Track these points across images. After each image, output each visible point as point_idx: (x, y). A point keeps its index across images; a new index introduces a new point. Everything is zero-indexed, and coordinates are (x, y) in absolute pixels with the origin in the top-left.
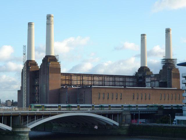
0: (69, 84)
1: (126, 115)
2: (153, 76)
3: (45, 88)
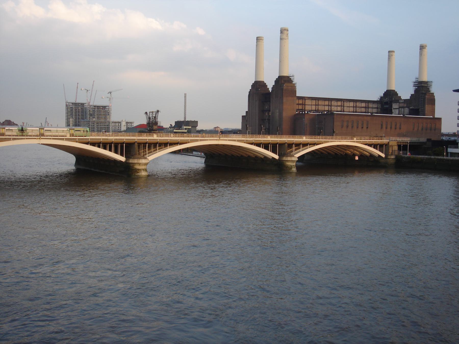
0: (302, 110)
1: (393, 146)
2: (402, 101)
3: (277, 114)
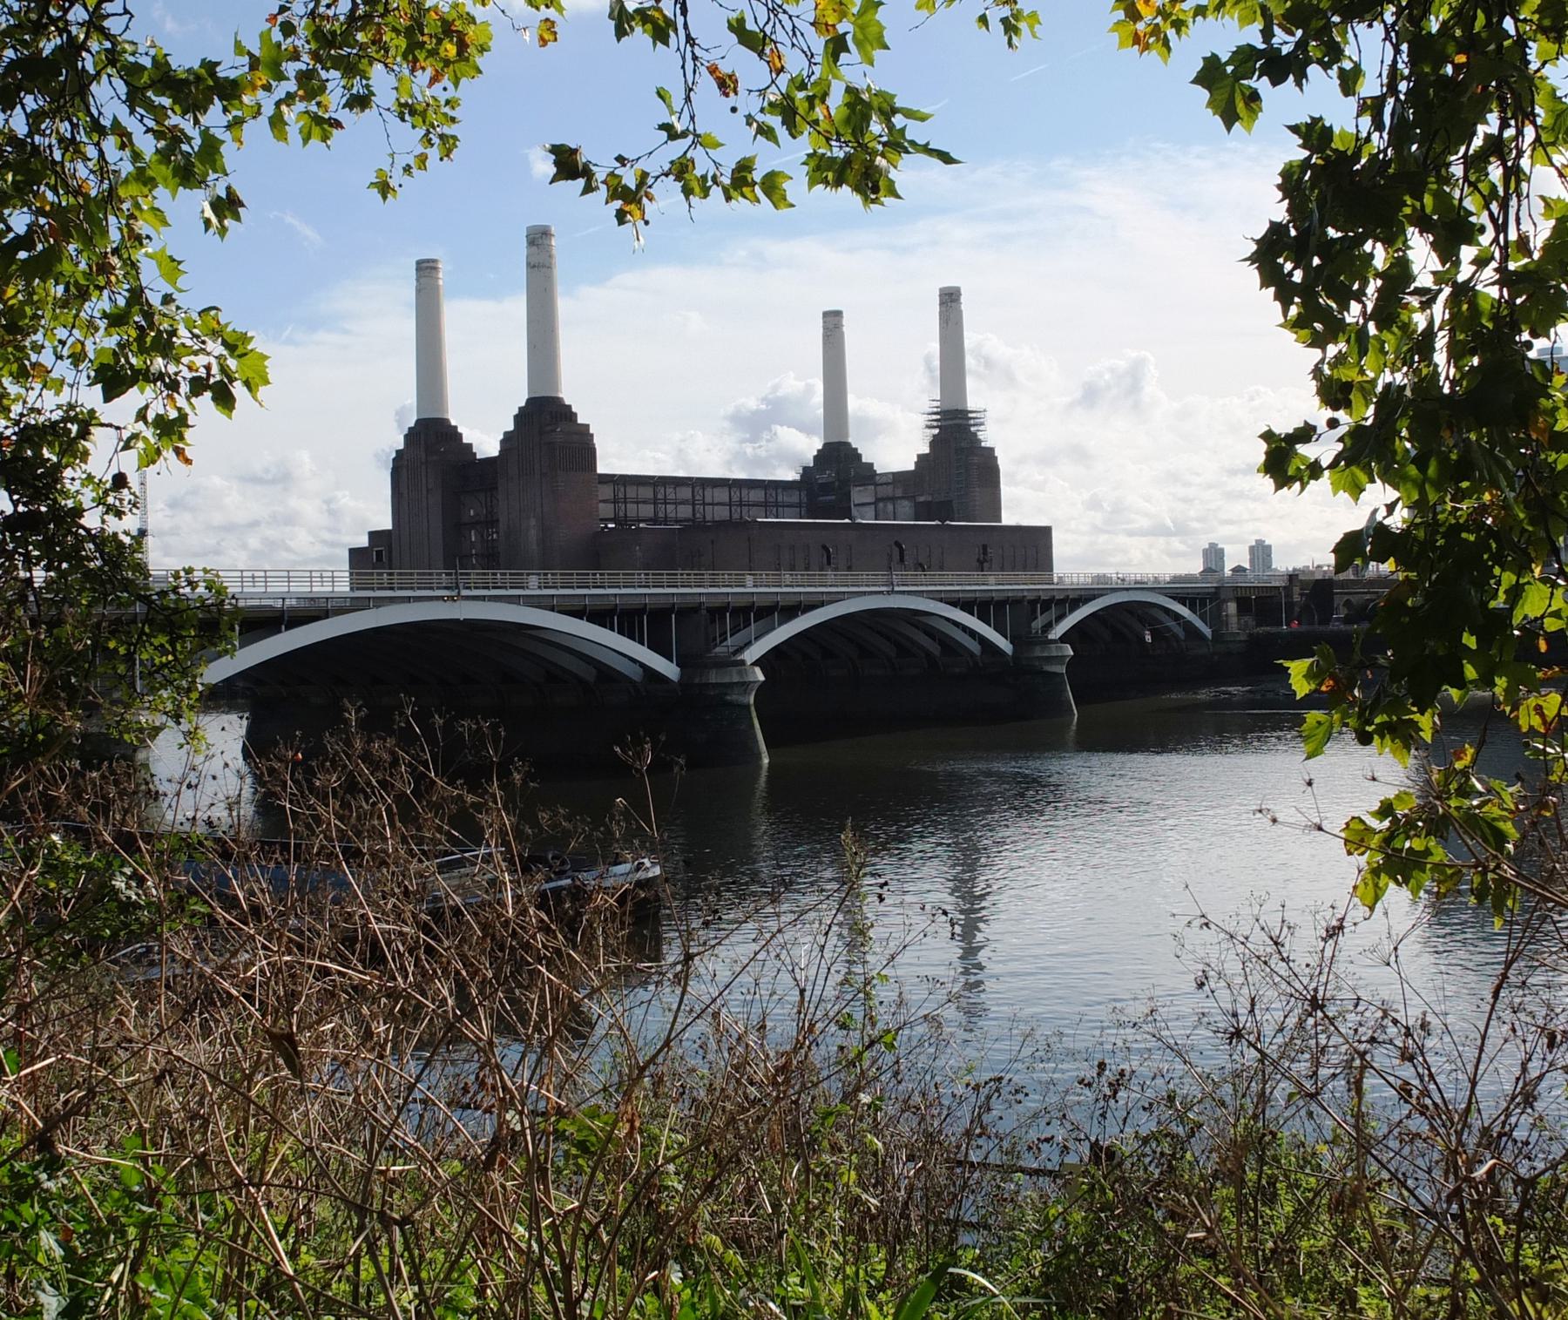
2: (884, 480)
